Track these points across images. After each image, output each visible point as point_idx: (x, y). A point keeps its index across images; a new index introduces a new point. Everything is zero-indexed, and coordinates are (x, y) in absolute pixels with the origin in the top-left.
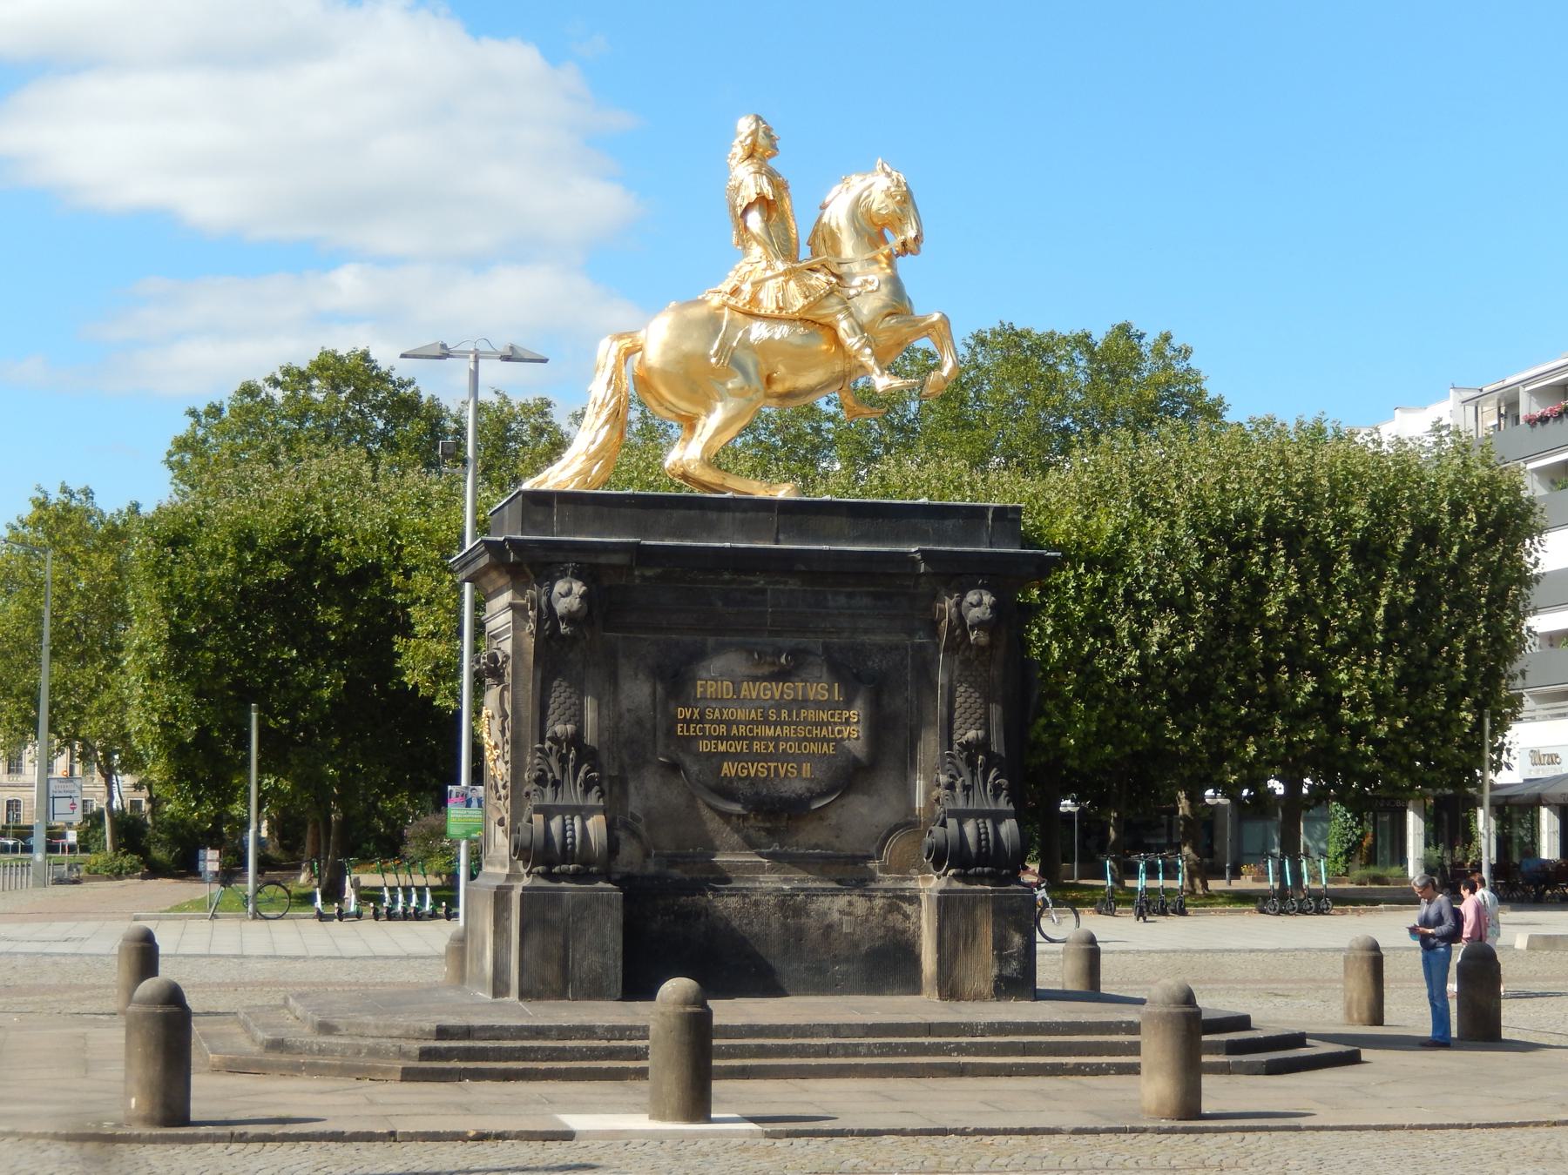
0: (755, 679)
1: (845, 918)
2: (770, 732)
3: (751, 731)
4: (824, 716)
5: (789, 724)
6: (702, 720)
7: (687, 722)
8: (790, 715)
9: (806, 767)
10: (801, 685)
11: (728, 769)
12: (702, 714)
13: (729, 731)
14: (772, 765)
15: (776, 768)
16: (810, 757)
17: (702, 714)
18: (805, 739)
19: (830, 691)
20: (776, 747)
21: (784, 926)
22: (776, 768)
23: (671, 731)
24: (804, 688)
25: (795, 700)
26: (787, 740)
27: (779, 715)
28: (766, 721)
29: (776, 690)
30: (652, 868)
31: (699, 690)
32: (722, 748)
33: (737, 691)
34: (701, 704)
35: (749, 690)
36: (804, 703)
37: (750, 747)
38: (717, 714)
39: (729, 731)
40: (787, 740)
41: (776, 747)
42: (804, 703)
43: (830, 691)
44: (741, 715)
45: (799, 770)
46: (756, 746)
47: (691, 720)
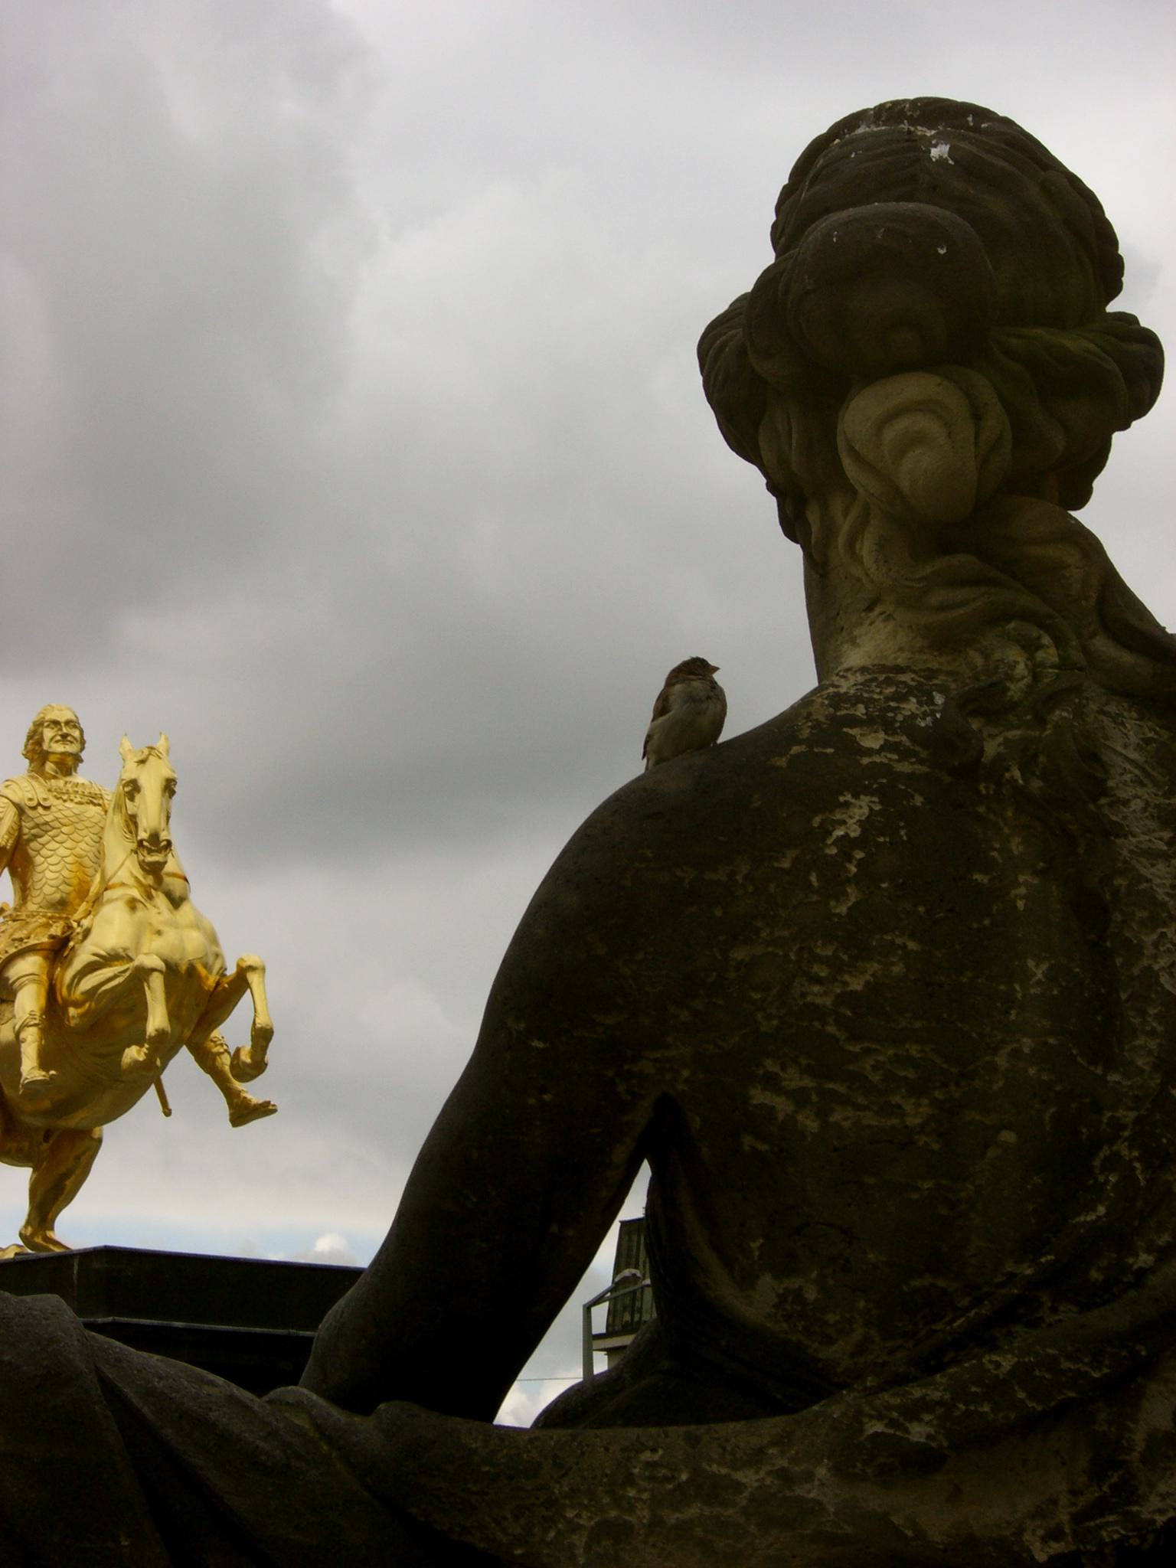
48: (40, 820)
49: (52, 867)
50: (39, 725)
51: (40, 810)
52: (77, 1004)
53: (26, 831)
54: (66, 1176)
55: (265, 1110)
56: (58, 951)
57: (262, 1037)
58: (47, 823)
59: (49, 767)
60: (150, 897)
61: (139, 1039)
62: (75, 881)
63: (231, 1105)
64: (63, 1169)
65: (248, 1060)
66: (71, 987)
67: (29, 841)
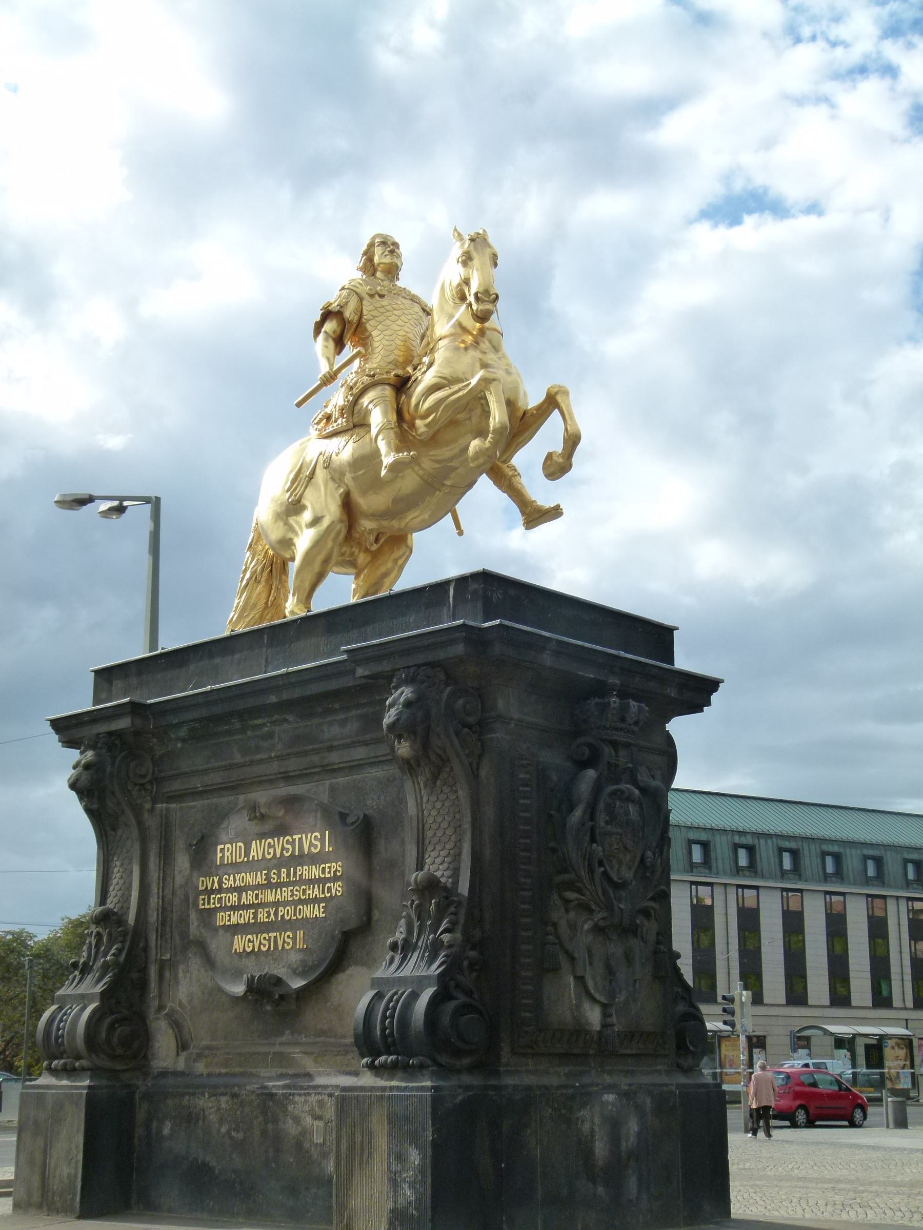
0: (262, 836)
1: (316, 1123)
2: (271, 897)
3: (257, 895)
4: (314, 871)
5: (286, 884)
6: (220, 890)
7: (209, 892)
8: (288, 875)
9: (300, 934)
10: (297, 837)
11: (240, 943)
12: (220, 882)
13: (239, 899)
14: (272, 935)
15: (275, 937)
16: (304, 923)
17: (220, 882)
18: (301, 902)
19: (322, 840)
20: (276, 914)
21: (264, 1133)
22: (275, 937)
23: (196, 904)
24: (300, 839)
25: (292, 855)
26: (285, 904)
27: (279, 877)
28: (269, 885)
29: (278, 846)
30: (181, 1065)
31: (219, 855)
32: (234, 920)
33: (247, 854)
34: (220, 873)
35: (257, 850)
36: (300, 859)
37: (255, 915)
38: (232, 882)
39: (239, 899)
40: (285, 904)
41: (276, 914)
42: (300, 859)
43: (322, 840)
44: (250, 878)
45: (294, 939)
46: (262, 916)
47: (212, 892)
48: (378, 305)
49: (385, 342)
50: (371, 245)
51: (377, 296)
52: (424, 417)
53: (365, 312)
54: (385, 575)
55: (555, 513)
56: (402, 385)
57: (572, 441)
58: (383, 307)
59: (378, 274)
60: (477, 343)
61: (482, 433)
62: (402, 348)
63: (523, 513)
64: (383, 570)
65: (561, 460)
66: (417, 405)
67: (368, 320)
